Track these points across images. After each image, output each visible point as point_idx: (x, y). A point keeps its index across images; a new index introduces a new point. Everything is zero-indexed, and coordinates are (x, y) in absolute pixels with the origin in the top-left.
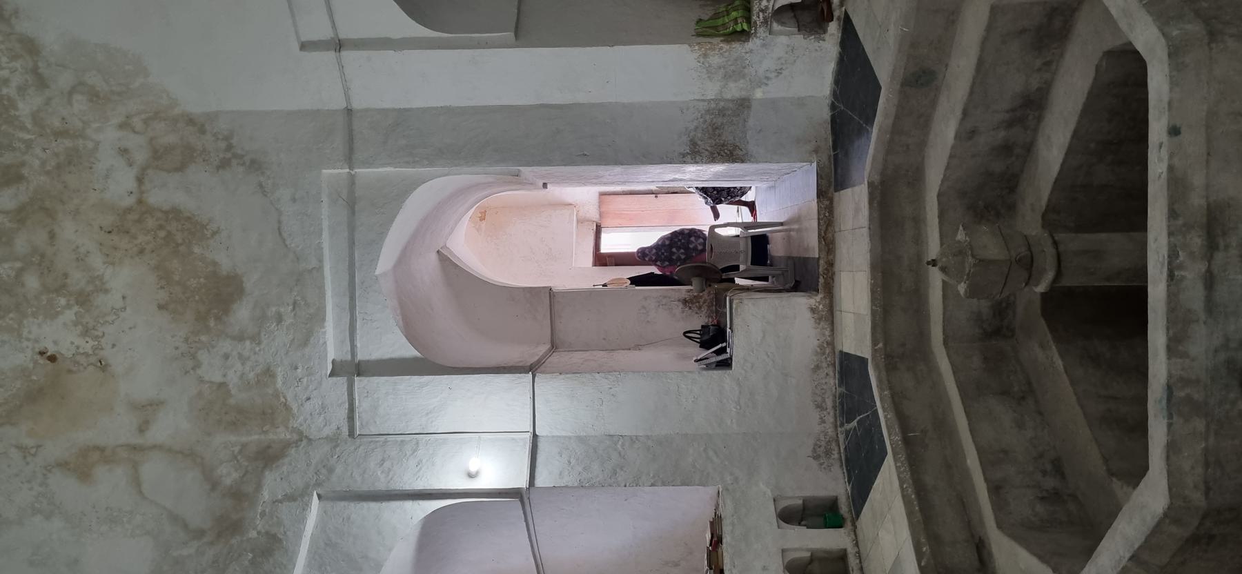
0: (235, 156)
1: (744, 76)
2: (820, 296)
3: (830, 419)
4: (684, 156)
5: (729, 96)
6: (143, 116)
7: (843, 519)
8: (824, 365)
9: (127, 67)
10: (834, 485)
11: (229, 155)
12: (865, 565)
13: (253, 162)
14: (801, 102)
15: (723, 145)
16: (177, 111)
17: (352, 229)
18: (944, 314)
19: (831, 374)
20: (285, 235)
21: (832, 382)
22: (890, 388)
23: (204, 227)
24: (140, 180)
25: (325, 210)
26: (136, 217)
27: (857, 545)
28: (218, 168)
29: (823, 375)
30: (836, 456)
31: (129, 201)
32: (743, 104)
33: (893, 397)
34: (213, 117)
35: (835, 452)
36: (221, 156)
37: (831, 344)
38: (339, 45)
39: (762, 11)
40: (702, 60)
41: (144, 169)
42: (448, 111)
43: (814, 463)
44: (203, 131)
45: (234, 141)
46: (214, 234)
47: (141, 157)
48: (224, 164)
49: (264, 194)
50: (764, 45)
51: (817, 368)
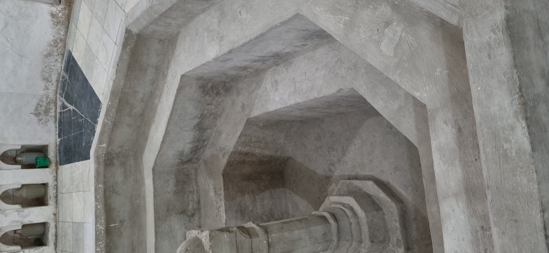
2: (61, 7)
3: (52, 88)
7: (50, 162)
8: (55, 54)
10: (48, 136)
12: (60, 196)
18: (159, 152)
19: (60, 60)
21: (59, 65)
22: (105, 183)
27: (56, 180)
29: (53, 60)
30: (53, 114)
33: (105, 191)
35: (53, 111)
37: (64, 42)
43: (35, 119)
51: (49, 55)
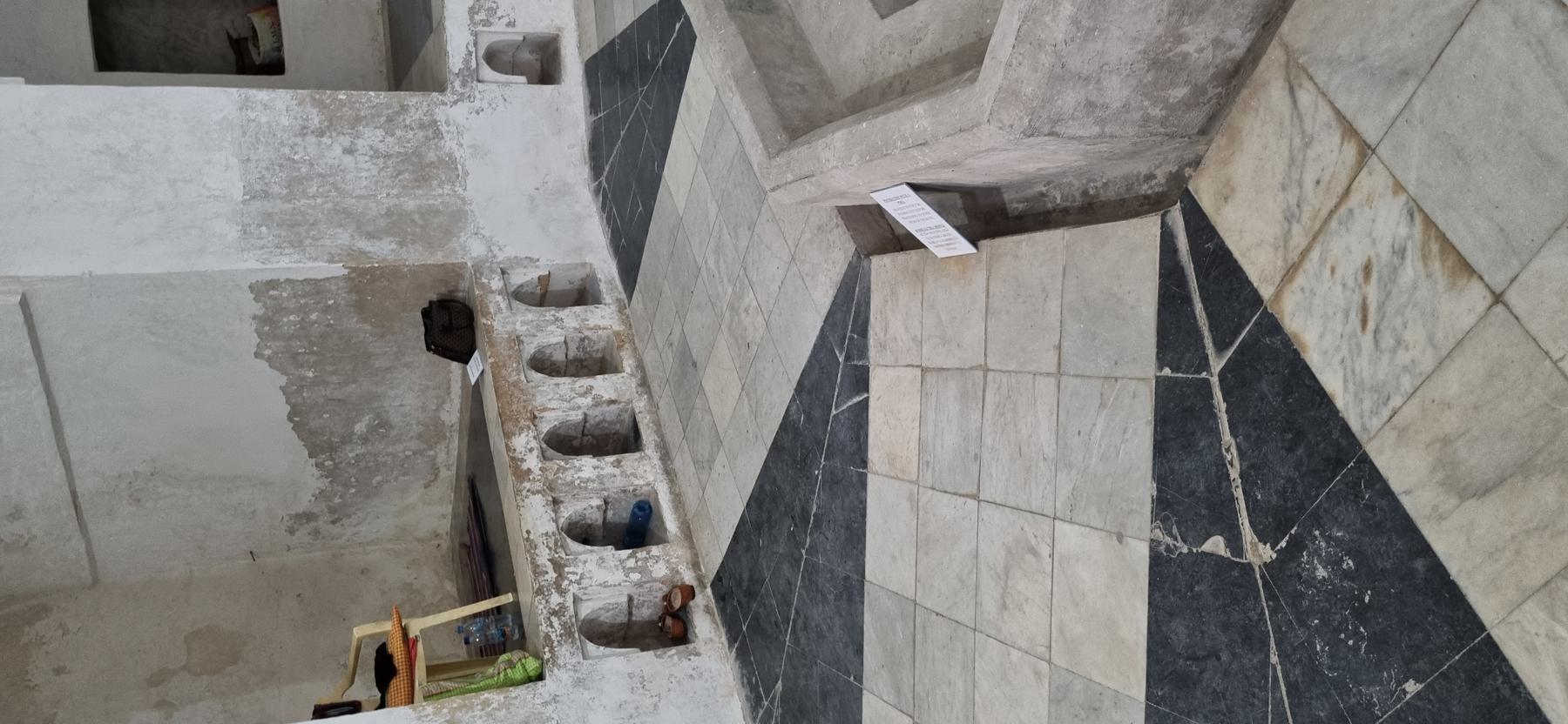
39: (555, 613)
50: (579, 683)
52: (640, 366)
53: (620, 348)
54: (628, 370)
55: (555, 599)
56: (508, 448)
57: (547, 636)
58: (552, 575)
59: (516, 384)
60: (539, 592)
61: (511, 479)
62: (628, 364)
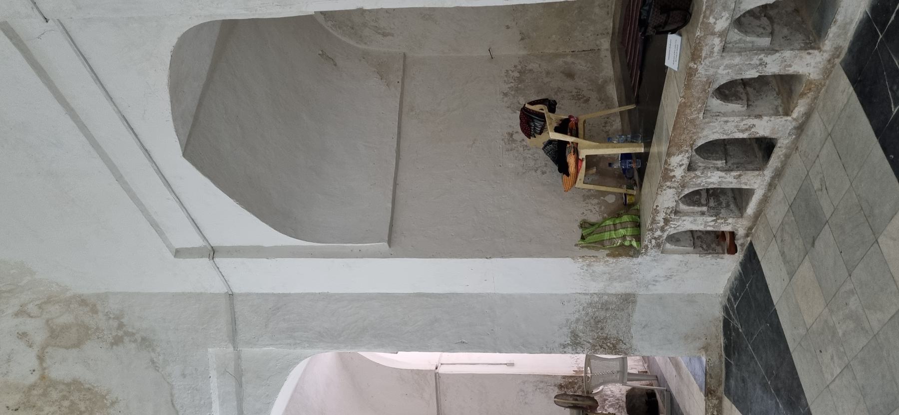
0: (127, 334)
1: (630, 279)
4: (564, 346)
5: (613, 292)
6: (37, 302)
9: (12, 272)
11: (120, 333)
13: (144, 339)
14: (691, 299)
15: (606, 339)
16: (68, 294)
17: (240, 400)
20: (178, 407)
23: (104, 397)
24: (41, 358)
25: (214, 383)
26: (41, 391)
28: (112, 344)
31: (33, 379)
32: (628, 300)
34: (103, 297)
36: (114, 334)
38: (213, 252)
39: (655, 238)
40: (585, 268)
41: (43, 349)
42: (326, 297)
44: (94, 311)
45: (125, 320)
46: (113, 403)
47: (39, 338)
48: (117, 341)
49: (156, 369)
52: (808, 115)
53: (802, 95)
54: (795, 115)
55: (658, 233)
56: (666, 162)
57: (647, 246)
58: (662, 224)
59: (692, 121)
60: (651, 230)
61: (659, 177)
62: (799, 110)
